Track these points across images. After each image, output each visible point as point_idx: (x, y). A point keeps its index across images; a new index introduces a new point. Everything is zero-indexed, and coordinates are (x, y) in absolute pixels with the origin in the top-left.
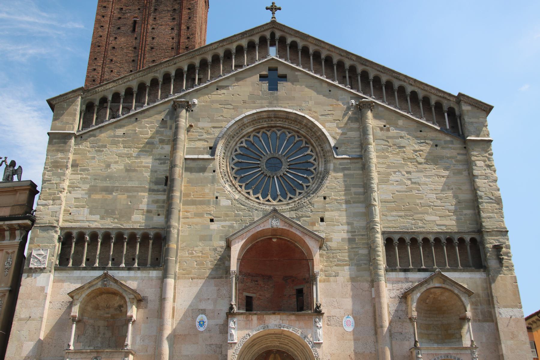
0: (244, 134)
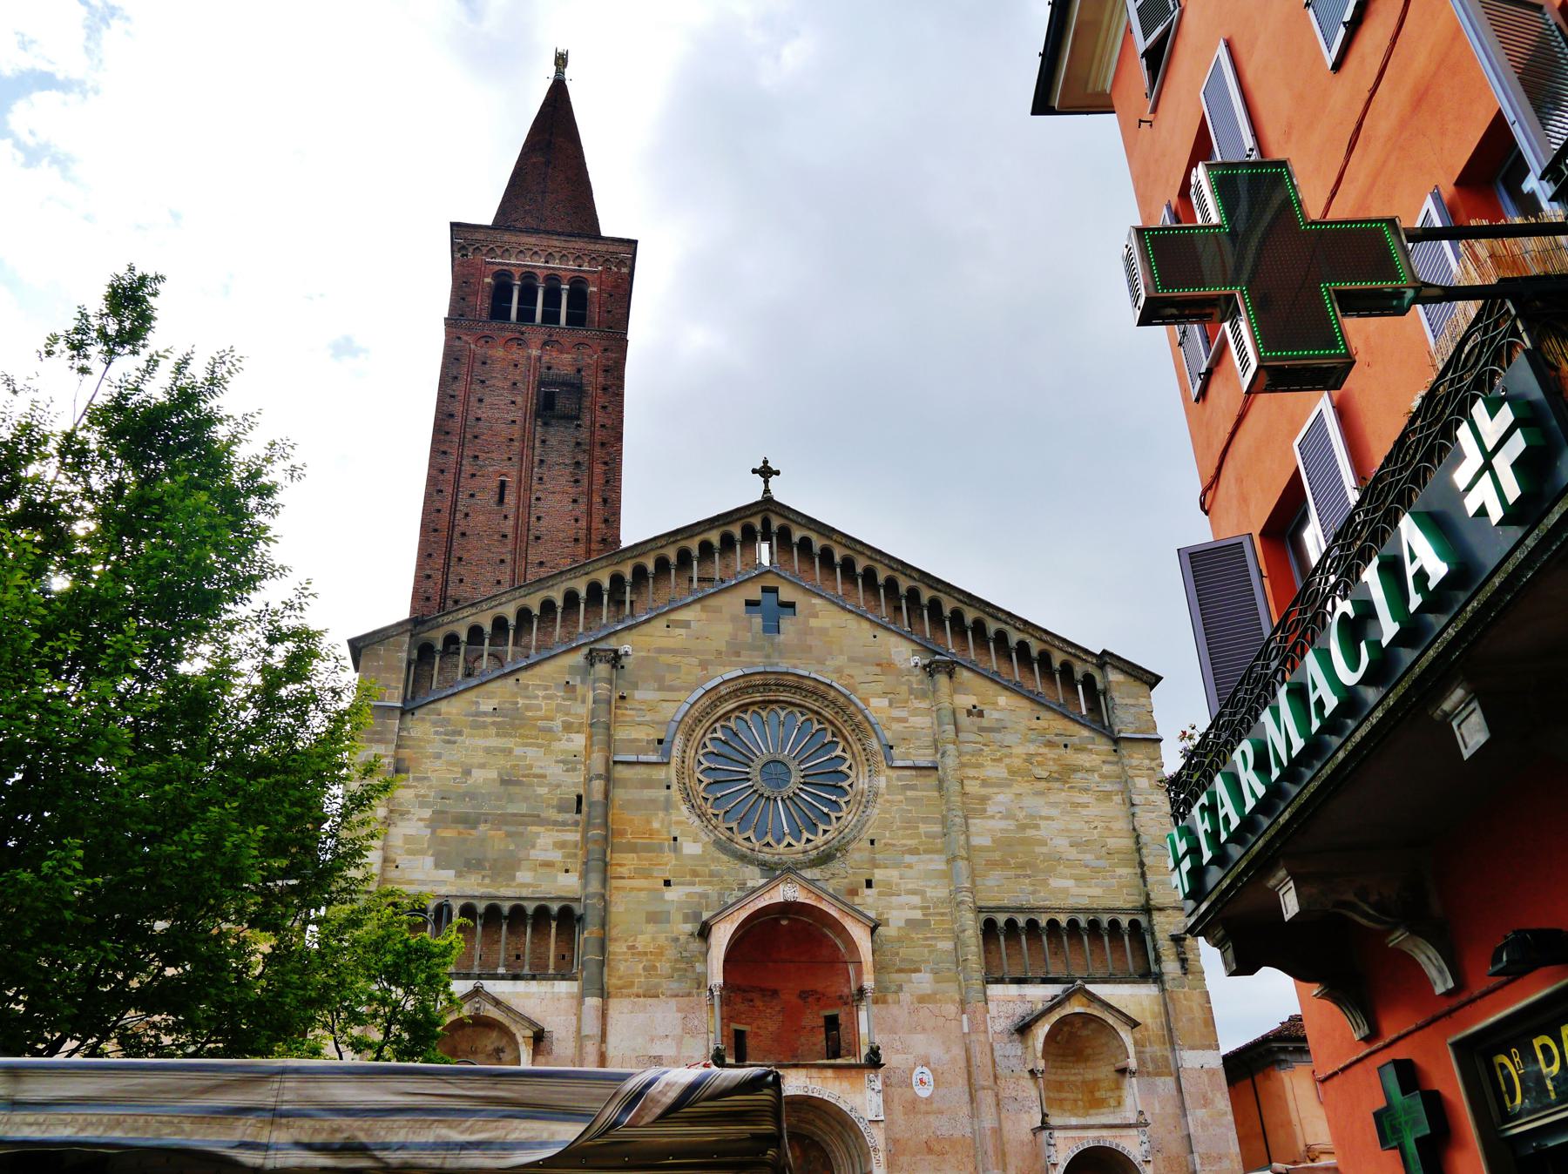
0: (718, 714)
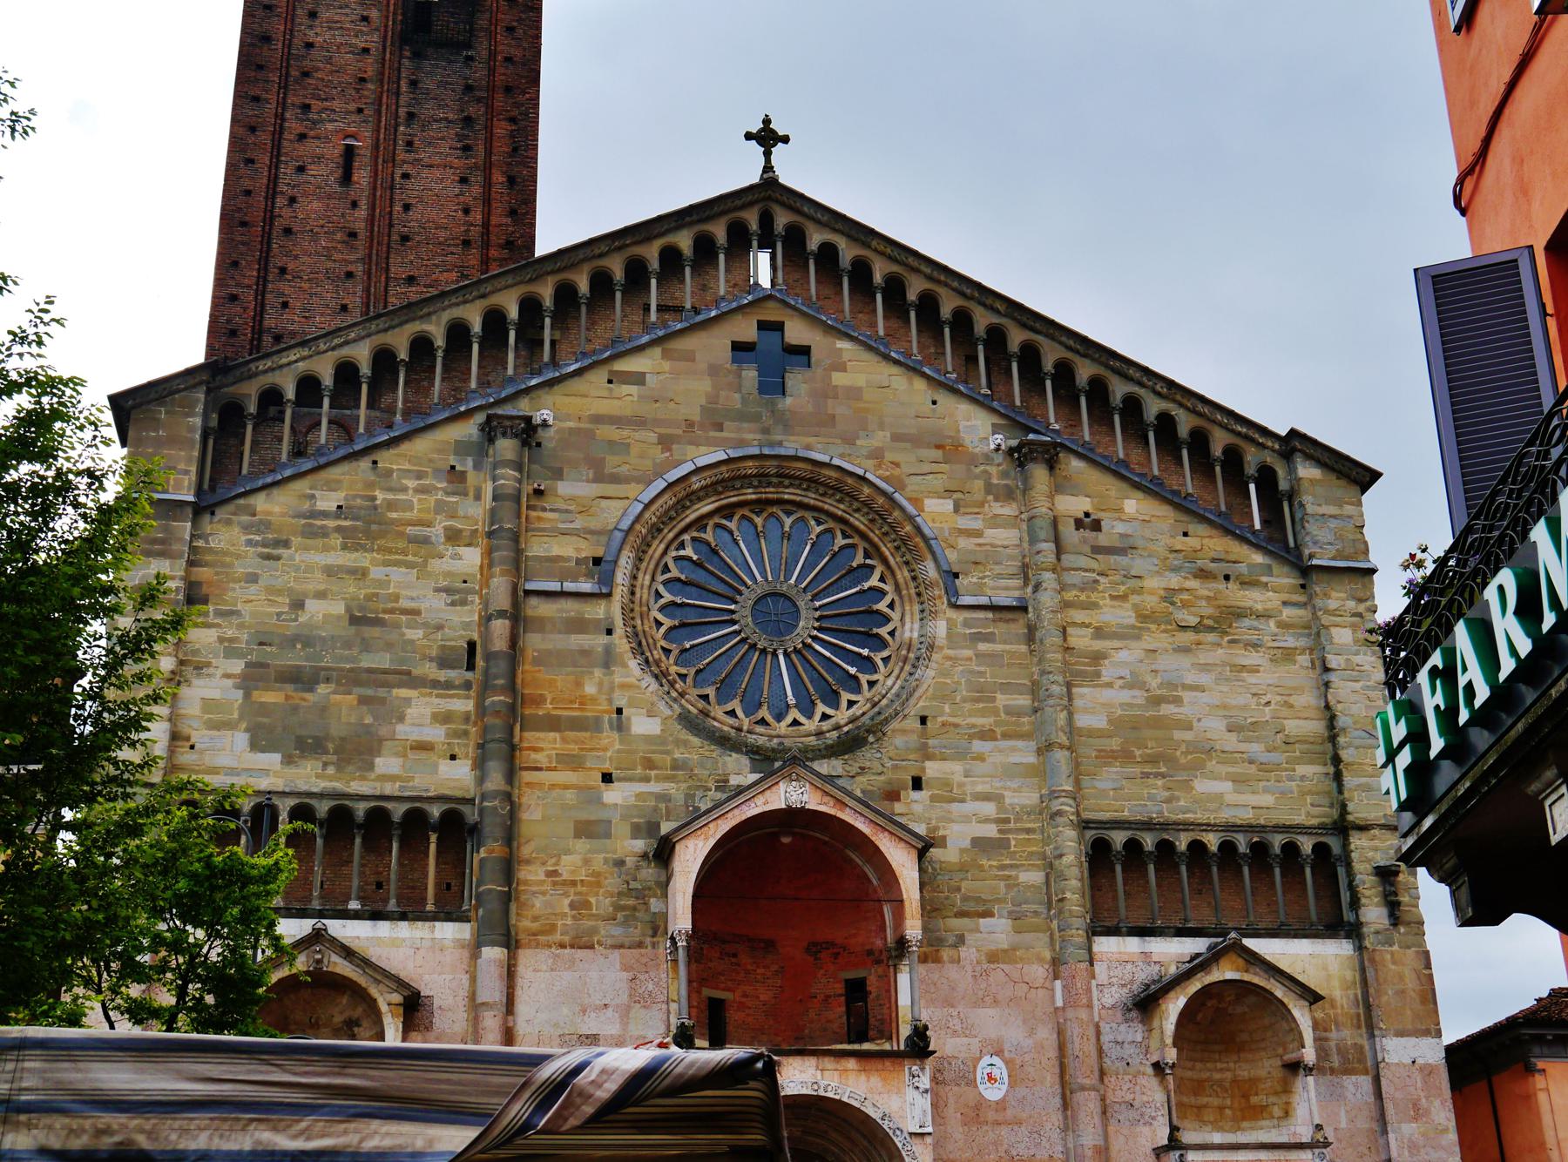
0: (688, 520)
